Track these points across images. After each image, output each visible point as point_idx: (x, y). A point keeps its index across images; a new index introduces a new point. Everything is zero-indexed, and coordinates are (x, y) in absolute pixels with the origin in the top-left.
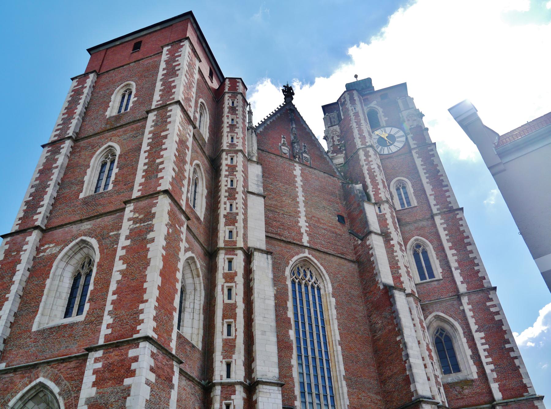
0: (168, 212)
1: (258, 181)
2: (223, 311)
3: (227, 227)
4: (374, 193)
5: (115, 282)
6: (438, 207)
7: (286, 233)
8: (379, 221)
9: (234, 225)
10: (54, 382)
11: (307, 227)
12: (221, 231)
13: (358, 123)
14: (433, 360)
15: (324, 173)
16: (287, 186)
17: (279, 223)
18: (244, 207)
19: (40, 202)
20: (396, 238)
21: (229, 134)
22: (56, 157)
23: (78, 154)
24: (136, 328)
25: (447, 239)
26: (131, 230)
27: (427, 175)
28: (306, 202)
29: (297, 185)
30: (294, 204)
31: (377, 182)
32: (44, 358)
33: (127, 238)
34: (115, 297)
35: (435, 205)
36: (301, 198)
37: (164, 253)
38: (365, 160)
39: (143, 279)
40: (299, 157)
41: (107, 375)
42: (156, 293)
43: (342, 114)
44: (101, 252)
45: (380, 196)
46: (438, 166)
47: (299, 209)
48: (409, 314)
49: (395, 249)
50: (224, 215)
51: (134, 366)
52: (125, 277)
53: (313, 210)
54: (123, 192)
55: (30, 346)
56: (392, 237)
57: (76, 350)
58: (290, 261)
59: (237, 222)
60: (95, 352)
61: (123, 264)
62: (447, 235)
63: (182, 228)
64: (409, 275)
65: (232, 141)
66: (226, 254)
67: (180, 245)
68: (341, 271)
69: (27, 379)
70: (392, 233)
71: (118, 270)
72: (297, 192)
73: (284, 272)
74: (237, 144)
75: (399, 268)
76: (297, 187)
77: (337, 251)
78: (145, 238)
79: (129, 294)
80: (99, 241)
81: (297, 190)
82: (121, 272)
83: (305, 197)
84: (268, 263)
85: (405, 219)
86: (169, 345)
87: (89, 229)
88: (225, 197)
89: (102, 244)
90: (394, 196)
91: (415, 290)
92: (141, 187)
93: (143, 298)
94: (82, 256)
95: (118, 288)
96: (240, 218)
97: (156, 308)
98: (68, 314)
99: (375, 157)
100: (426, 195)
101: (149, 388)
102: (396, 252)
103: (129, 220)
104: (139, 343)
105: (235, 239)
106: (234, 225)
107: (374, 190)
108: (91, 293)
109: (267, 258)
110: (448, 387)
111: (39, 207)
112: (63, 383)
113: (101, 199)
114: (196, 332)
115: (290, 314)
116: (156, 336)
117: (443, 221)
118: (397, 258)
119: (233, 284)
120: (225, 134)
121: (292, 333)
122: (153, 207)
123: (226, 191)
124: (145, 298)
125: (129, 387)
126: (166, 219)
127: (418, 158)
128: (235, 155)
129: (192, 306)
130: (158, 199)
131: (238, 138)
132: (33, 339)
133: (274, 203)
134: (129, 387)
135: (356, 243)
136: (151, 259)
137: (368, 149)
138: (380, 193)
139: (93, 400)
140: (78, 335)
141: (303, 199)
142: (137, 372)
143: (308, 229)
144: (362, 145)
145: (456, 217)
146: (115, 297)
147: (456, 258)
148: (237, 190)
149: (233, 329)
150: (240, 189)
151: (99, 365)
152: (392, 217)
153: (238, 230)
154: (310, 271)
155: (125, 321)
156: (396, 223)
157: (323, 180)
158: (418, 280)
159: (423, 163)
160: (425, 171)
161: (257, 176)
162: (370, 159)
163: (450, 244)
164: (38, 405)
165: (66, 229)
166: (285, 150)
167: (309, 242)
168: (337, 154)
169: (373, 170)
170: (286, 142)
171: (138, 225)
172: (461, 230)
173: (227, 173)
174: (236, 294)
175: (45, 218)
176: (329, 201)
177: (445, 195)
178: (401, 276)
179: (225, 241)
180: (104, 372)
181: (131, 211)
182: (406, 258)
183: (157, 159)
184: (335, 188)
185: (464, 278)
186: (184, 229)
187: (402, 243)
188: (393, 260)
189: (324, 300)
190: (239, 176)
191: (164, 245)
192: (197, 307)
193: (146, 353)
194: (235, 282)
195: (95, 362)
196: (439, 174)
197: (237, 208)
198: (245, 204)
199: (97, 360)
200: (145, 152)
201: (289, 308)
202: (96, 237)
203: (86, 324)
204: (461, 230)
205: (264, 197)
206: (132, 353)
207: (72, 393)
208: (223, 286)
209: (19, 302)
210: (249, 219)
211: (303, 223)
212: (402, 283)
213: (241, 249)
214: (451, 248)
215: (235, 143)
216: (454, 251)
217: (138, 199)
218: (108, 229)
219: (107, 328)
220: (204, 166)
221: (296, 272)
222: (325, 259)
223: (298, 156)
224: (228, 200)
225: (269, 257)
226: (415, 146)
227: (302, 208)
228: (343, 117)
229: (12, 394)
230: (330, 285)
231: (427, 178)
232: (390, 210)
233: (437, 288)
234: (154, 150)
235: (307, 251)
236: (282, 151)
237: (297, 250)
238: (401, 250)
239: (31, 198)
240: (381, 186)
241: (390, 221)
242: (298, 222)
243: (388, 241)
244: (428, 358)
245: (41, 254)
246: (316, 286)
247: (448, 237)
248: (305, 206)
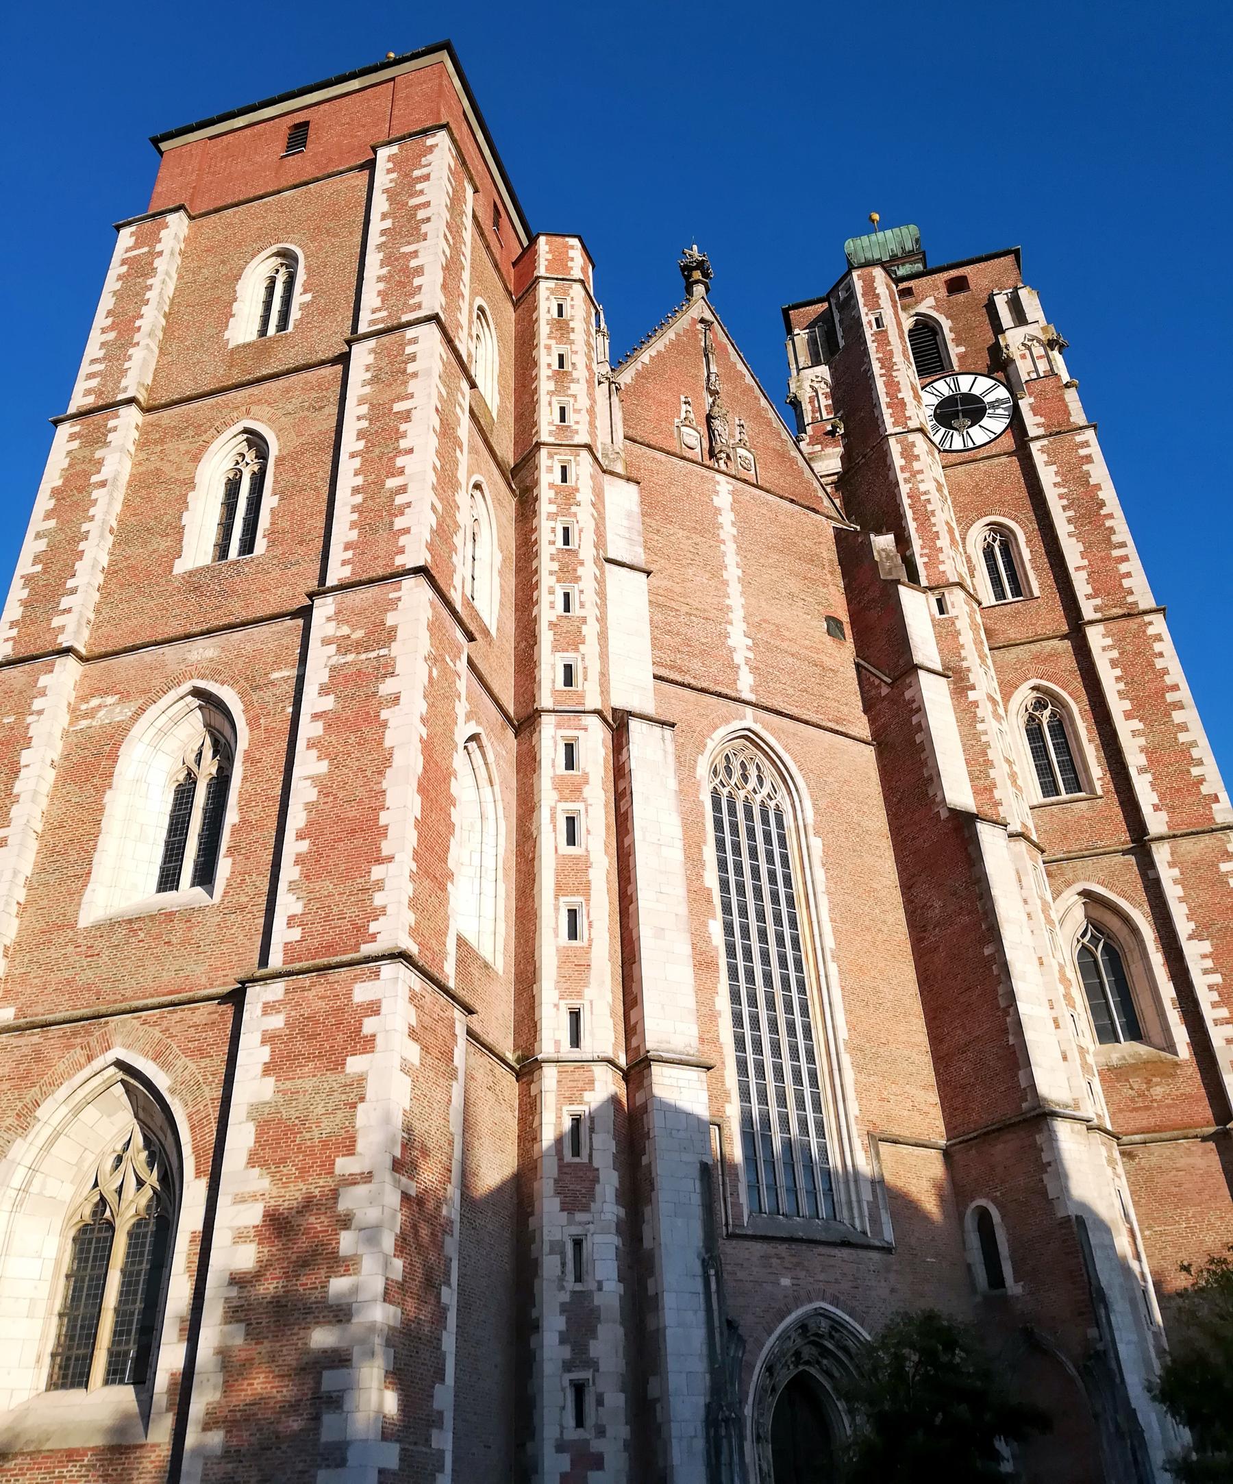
0: (428, 625)
1: (630, 529)
2: (557, 875)
3: (558, 655)
4: (926, 559)
5: (301, 807)
6: (1098, 601)
7: (696, 665)
8: (939, 637)
9: (577, 650)
10: (154, 1060)
11: (749, 649)
12: (543, 666)
13: (888, 365)
14: (1074, 1007)
15: (792, 501)
16: (698, 539)
17: (678, 639)
18: (599, 602)
19: (66, 579)
20: (984, 682)
21: (555, 399)
22: (98, 455)
23: (159, 448)
24: (366, 928)
25: (1118, 691)
26: (333, 669)
27: (1071, 513)
28: (745, 582)
29: (723, 535)
30: (717, 589)
31: (935, 529)
32: (119, 997)
33: (324, 691)
34: (304, 846)
35: (1088, 597)
36: (732, 573)
37: (424, 732)
38: (903, 469)
39: (377, 800)
40: (728, 457)
41: (300, 1046)
42: (412, 837)
43: (840, 334)
44: (253, 723)
45: (942, 568)
46: (1100, 489)
47: (728, 602)
48: (1016, 888)
49: (980, 713)
50: (551, 623)
51: (369, 1025)
52: (327, 795)
53: (763, 604)
54: (297, 563)
55: (78, 965)
56: (972, 682)
57: (204, 980)
58: (708, 741)
59: (583, 643)
60: (263, 988)
61: (319, 758)
62: (1118, 679)
63: (458, 662)
64: (1014, 782)
65: (563, 419)
66: (559, 726)
67: (456, 710)
68: (837, 768)
69: (78, 1049)
70: (973, 669)
71: (307, 774)
72: (724, 554)
73: (694, 768)
74: (575, 427)
75: (989, 764)
76: (723, 542)
77: (824, 713)
78: (375, 694)
79: (340, 840)
80: (242, 695)
81: (723, 547)
82: (314, 779)
83: (744, 567)
84: (665, 751)
85: (1004, 632)
86: (442, 968)
87: (211, 660)
88: (551, 573)
89: (252, 703)
90: (977, 567)
91: (1031, 825)
92: (349, 554)
93: (379, 850)
94: (193, 731)
95: (310, 823)
96: (590, 631)
97: (413, 877)
98: (169, 880)
99: (929, 460)
100: (1066, 569)
101: (408, 1080)
102: (983, 721)
103: (326, 642)
104: (379, 967)
105: (580, 688)
106: (577, 650)
107: (926, 551)
108: (232, 834)
109: (663, 739)
110: (1113, 1075)
111: (63, 595)
112: (179, 1063)
113: (237, 579)
114: (488, 926)
115: (711, 879)
116: (414, 949)
117: (1109, 641)
118: (984, 738)
119: (579, 806)
120: (544, 398)
121: (716, 928)
122: (387, 611)
123: (552, 559)
124: (385, 853)
125: (361, 1080)
126: (424, 644)
127: (1047, 464)
128: (572, 458)
129: (476, 861)
130: (400, 589)
131: (575, 411)
132: (84, 948)
133: (665, 583)
134: (361, 1080)
135: (873, 692)
136: (396, 751)
137: (912, 437)
138: (943, 562)
139: (267, 1110)
140: (208, 941)
141: (739, 572)
142: (379, 1041)
143: (751, 655)
144: (895, 424)
145: (1144, 632)
146: (304, 846)
147: (1142, 741)
148: (581, 556)
149: (582, 922)
150: (587, 552)
151: (277, 1022)
152: (974, 626)
153: (587, 663)
154: (758, 766)
155: (335, 909)
156: (982, 642)
157: (789, 521)
158: (1037, 796)
159: (1059, 479)
160: (1065, 502)
161: (629, 515)
162: (917, 466)
163: (1127, 705)
164: (109, 1116)
165: (146, 655)
166: (693, 437)
167: (753, 690)
168: (825, 446)
169: (923, 498)
171: (350, 657)
172: (1158, 667)
173: (553, 508)
174: (588, 832)
175: (85, 624)
177: (1118, 570)
178: (994, 785)
179: (555, 692)
180: (291, 1038)
181: (329, 619)
182: (1008, 738)
183: (388, 477)
184: (820, 543)
185: (1162, 797)
186: (462, 666)
187: (998, 697)
188: (974, 742)
189: (792, 841)
190: (584, 517)
191: (424, 712)
192: (489, 862)
193: (400, 994)
194: (584, 800)
195: (265, 1013)
196: (1103, 512)
197: (582, 605)
198: (602, 594)
199: (268, 1008)
200: (353, 456)
201: (707, 863)
202: (233, 682)
203: (226, 911)
204: (1158, 667)
205: (649, 573)
206: (362, 993)
207: (206, 1089)
208: (553, 811)
209: (35, 851)
210: (611, 634)
211: (738, 638)
212: (997, 804)
213: (598, 712)
214: (1128, 716)
215: (572, 424)
216: (1136, 724)
217: (342, 587)
218: (266, 663)
219: (290, 925)
220: (492, 486)
221: (721, 769)
222: (794, 734)
223: (723, 455)
224: (558, 581)
225: (668, 732)
226: (1041, 431)
227: (736, 599)
228: (842, 343)
229: (44, 1088)
230: (808, 804)
231: (1069, 521)
232: (966, 608)
233: (1087, 819)
234: (377, 451)
235: (749, 710)
236: (681, 442)
237: (724, 710)
238: (995, 714)
239: (39, 568)
240: (944, 542)
241: (967, 638)
242: (727, 636)
243: (959, 693)
244: (1063, 1003)
245: (84, 723)
246: (772, 804)
247: (1121, 686)
248: (743, 593)
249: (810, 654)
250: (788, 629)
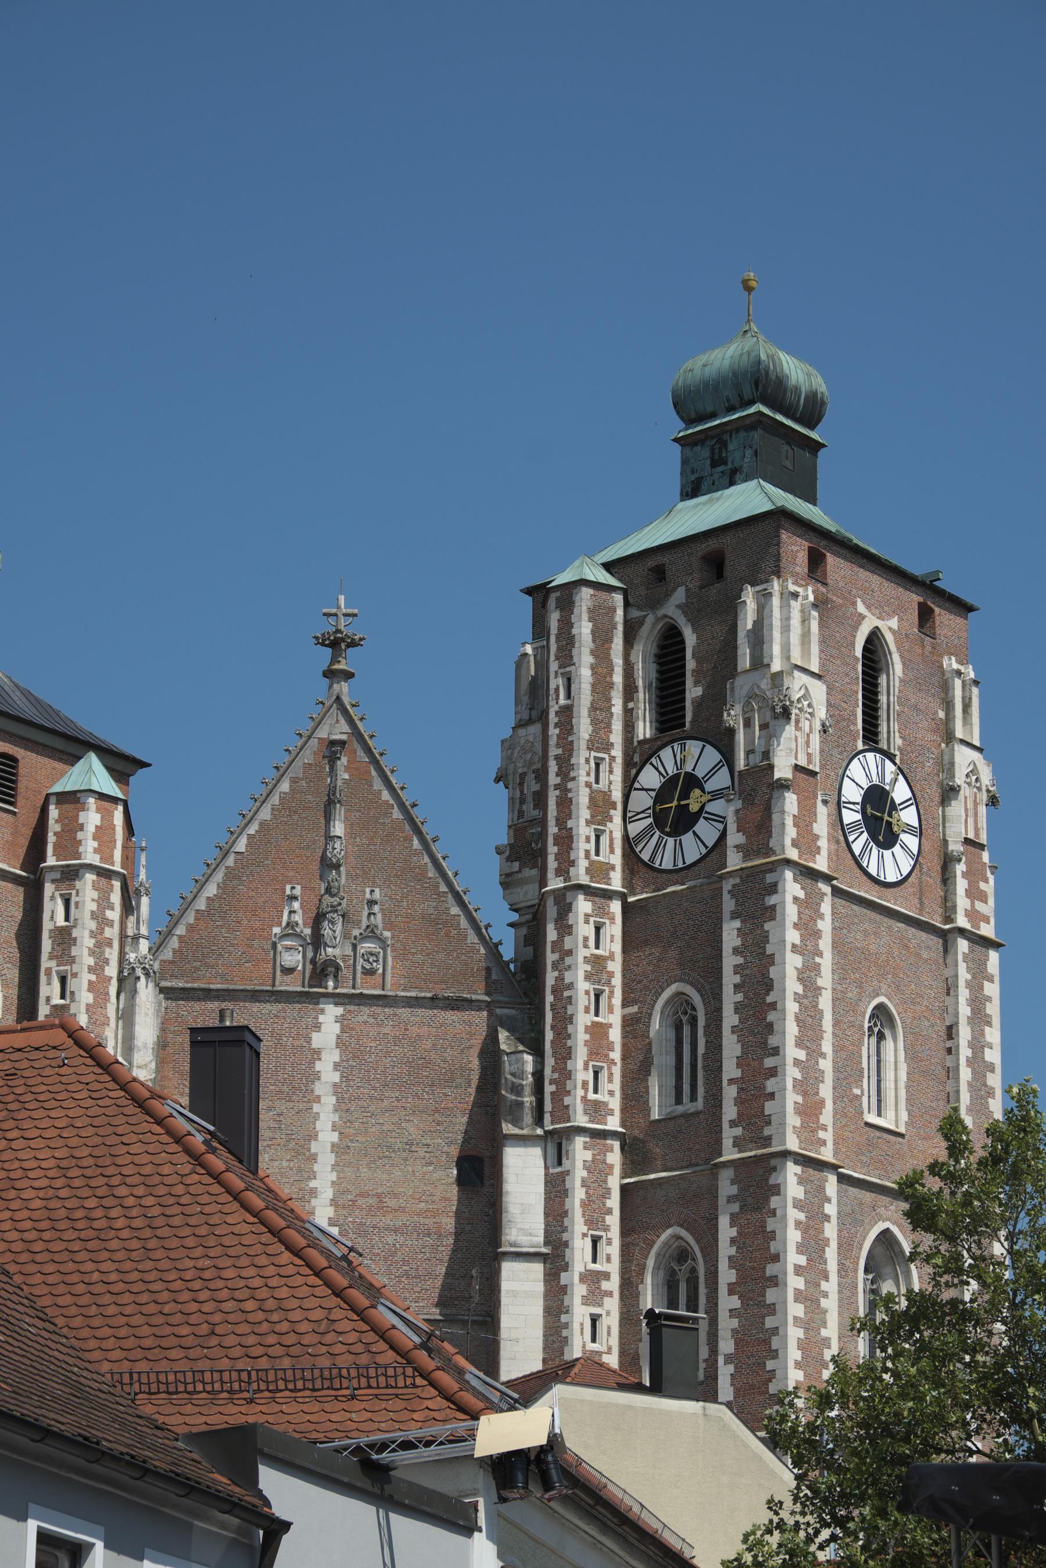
29: (319, 1089)
36: (326, 1136)
47: (312, 1184)
72: (316, 1117)
81: (316, 1108)
141: (335, 1137)
170: (298, 918)
176: (437, 1111)
249: (422, 1220)
250: (396, 1196)
